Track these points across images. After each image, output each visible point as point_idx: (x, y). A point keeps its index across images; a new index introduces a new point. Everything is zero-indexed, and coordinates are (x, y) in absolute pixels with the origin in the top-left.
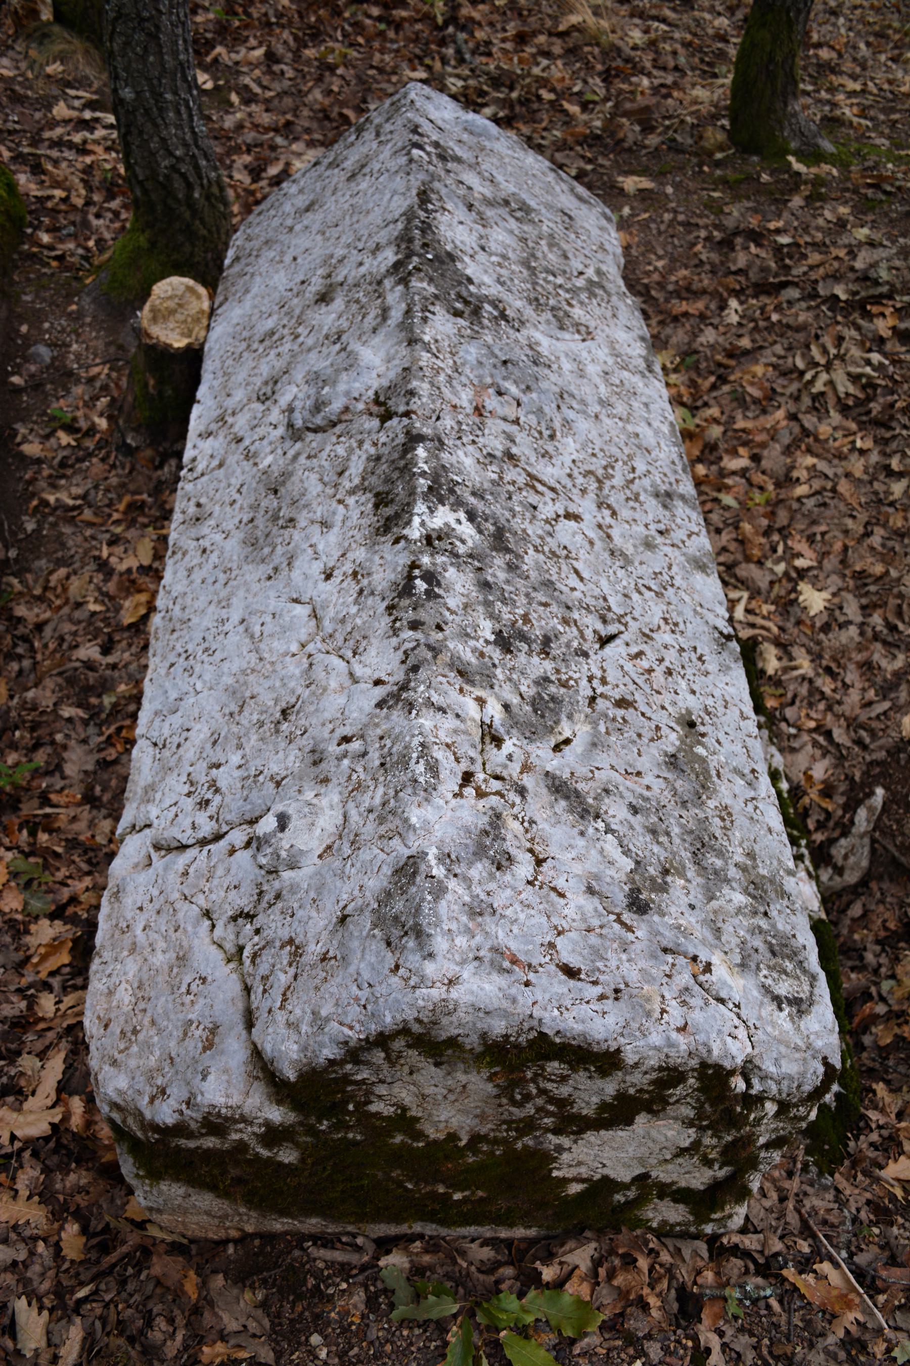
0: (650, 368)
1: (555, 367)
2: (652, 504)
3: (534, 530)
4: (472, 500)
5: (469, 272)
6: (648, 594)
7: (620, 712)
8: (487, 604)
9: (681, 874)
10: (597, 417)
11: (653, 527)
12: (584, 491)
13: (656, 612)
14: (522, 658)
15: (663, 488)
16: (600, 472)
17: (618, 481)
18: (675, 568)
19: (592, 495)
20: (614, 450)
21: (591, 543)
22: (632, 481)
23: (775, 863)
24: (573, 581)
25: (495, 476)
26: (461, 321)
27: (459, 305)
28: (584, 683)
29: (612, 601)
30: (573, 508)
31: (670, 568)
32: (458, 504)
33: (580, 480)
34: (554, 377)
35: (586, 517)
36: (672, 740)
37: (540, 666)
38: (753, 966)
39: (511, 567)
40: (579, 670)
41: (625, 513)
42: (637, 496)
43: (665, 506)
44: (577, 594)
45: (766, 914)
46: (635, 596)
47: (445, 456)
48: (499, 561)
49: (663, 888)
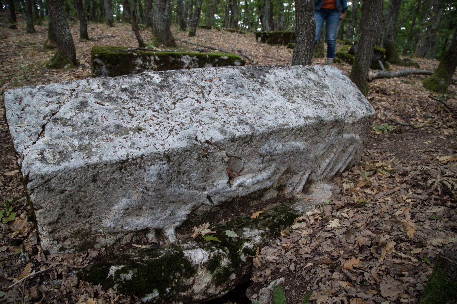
23: (101, 153)
38: (51, 147)
45: (75, 151)
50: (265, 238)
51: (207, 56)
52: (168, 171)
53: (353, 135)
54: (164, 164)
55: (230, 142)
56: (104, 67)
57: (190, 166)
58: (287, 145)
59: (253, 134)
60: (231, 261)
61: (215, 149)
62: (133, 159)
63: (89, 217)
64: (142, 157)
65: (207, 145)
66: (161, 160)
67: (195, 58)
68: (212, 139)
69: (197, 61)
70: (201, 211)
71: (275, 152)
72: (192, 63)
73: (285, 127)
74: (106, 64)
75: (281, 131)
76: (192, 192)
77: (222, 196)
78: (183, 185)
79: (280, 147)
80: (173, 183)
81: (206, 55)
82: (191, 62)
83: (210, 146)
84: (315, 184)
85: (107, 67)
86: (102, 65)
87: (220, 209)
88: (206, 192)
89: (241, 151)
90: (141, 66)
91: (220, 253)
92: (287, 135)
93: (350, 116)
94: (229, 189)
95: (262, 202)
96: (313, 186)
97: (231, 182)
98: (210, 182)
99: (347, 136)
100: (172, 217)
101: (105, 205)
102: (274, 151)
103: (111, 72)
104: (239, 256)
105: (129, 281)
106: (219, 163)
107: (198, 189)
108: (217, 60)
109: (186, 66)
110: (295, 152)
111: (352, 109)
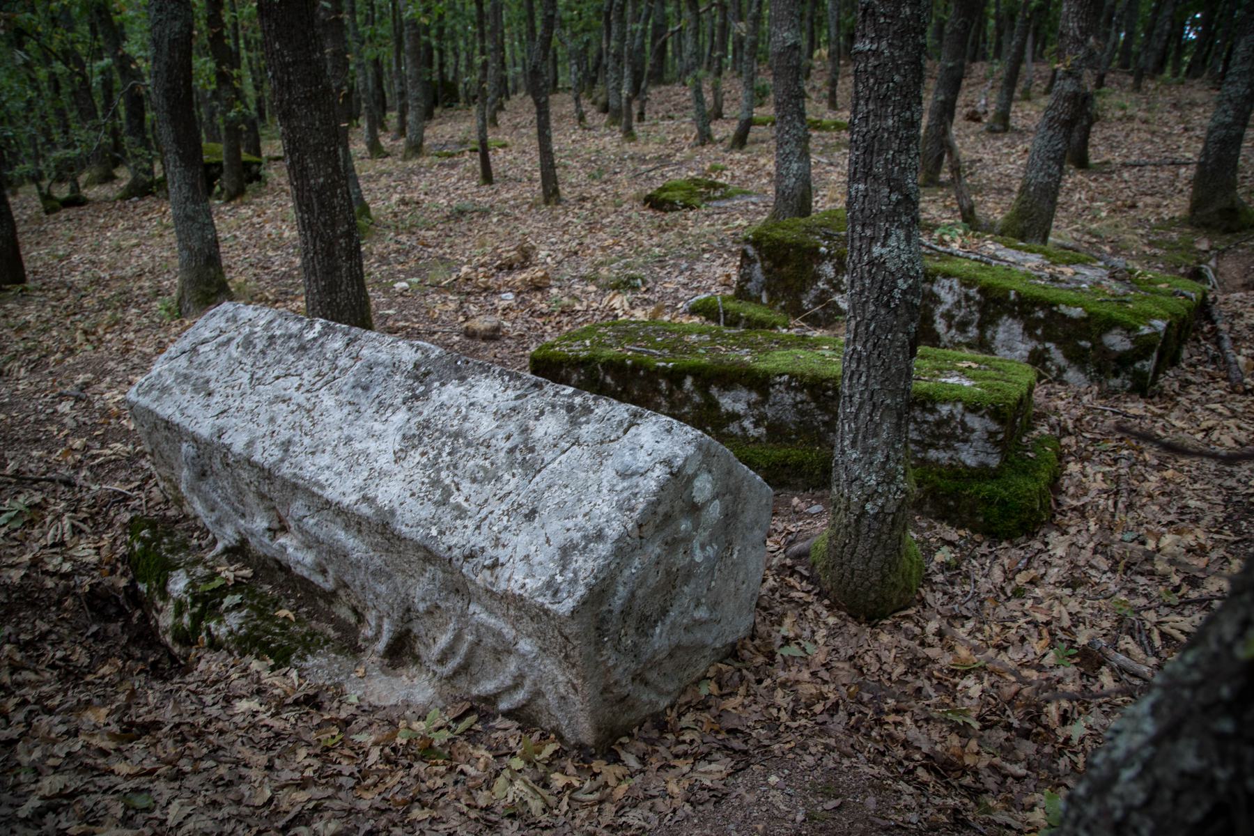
0: (365, 499)
1: (377, 416)
5: (449, 386)
9: (187, 368)
11: (277, 429)
12: (308, 400)
13: (248, 405)
15: (291, 449)
20: (318, 428)
24: (276, 373)
26: (410, 367)
27: (423, 369)
29: (261, 387)
30: (303, 389)
32: (321, 335)
33: (313, 400)
34: (370, 411)
35: (296, 394)
36: (212, 385)
37: (260, 347)
39: (292, 349)
40: (249, 361)
41: (290, 418)
42: (293, 428)
46: (257, 399)
51: (1012, 292)
56: (759, 265)
67: (973, 292)
69: (978, 303)
72: (963, 304)
73: (315, 489)
74: (763, 260)
79: (312, 521)
81: (1007, 291)
82: (959, 302)
84: (421, 672)
85: (763, 267)
86: (755, 261)
90: (829, 282)
93: (484, 567)
96: (414, 670)
97: (278, 535)
103: (768, 279)
107: (236, 510)
108: (1041, 314)
109: (942, 309)
111: (502, 554)
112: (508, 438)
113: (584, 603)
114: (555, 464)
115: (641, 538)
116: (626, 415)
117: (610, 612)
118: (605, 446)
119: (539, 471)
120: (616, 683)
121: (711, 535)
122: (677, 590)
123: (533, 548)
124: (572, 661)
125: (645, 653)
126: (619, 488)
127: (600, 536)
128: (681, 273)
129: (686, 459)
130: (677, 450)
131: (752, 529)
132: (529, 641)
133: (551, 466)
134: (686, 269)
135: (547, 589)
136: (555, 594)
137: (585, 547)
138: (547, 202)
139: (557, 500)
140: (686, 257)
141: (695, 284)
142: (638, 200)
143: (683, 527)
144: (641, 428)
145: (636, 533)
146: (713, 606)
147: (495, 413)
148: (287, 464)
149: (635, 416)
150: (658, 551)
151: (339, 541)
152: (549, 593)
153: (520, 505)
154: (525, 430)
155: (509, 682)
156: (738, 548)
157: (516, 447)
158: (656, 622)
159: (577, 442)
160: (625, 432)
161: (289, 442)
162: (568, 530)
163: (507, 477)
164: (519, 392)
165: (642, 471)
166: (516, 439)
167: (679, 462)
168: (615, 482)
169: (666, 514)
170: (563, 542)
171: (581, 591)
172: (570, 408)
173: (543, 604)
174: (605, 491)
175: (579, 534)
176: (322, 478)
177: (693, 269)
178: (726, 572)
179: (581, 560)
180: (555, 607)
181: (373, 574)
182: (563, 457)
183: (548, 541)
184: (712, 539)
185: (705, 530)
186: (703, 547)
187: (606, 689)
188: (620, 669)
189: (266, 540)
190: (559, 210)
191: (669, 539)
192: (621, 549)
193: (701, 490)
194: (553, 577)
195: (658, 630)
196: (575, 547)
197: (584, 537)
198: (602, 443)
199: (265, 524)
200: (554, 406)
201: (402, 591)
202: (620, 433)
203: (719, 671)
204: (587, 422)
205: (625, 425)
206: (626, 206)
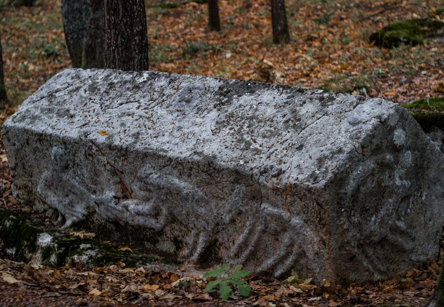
0: (195, 153)
1: (197, 115)
2: (136, 130)
3: (137, 96)
4: (149, 82)
6: (108, 119)
7: (84, 103)
8: (121, 82)
9: (49, 105)
10: (173, 123)
13: (102, 119)
14: (106, 87)
15: (140, 137)
16: (152, 119)
17: (147, 123)
18: (112, 129)
19: (145, 115)
21: (129, 109)
22: (145, 127)
24: (120, 102)
25: (156, 89)
26: (216, 89)
28: (94, 98)
30: (141, 108)
31: (113, 128)
32: (148, 79)
33: (150, 112)
34: (192, 114)
37: (103, 90)
39: (128, 89)
40: (97, 98)
41: (135, 123)
43: (134, 135)
44: (116, 102)
46: (109, 116)
47: (164, 78)
48: (131, 86)
49: (49, 101)
50: (90, 261)
52: (62, 155)
53: (285, 214)
54: (62, 148)
55: (108, 148)
57: (81, 160)
58: (164, 179)
59: (127, 148)
60: (57, 260)
61: (97, 150)
62: (45, 135)
63: (31, 176)
64: (51, 135)
65: (91, 144)
66: (61, 144)
68: (96, 139)
70: (97, 219)
71: (147, 180)
73: (161, 153)
75: (157, 157)
76: (81, 188)
77: (108, 210)
78: (77, 178)
79: (155, 176)
80: (71, 172)
83: (94, 147)
87: (116, 230)
88: (93, 196)
89: (120, 164)
91: (54, 247)
92: (167, 166)
93: (273, 176)
94: (113, 205)
95: (157, 249)
98: (99, 187)
99: (269, 209)
100: (70, 207)
101: (38, 170)
102: (146, 177)
104: (65, 262)
105: (6, 228)
106: (102, 168)
107: (89, 189)
110: (174, 192)
112: (284, 116)
113: (332, 182)
114: (314, 125)
115: (363, 155)
116: (355, 99)
117: (346, 194)
118: (342, 114)
119: (304, 129)
120: (348, 242)
121: (406, 174)
122: (385, 200)
123: (302, 161)
124: (323, 222)
125: (365, 230)
126: (350, 130)
127: (340, 151)
128: (401, 85)
129: (389, 115)
130: (384, 111)
131: (435, 184)
132: (298, 217)
133: (311, 126)
134: (406, 82)
135: (311, 178)
136: (315, 179)
137: (332, 156)
138: (276, 41)
139: (315, 139)
140: (406, 74)
141: (413, 92)
142: (364, 39)
143: (388, 157)
144: (363, 105)
145: (360, 150)
146: (410, 226)
147: (275, 106)
148: (138, 144)
149: (360, 100)
150: (373, 166)
151: (175, 184)
152: (312, 180)
153: (293, 145)
154: (294, 112)
155: (283, 253)
156: (425, 193)
157: (289, 120)
158: (372, 215)
159: (326, 114)
160: (354, 107)
161: (138, 133)
162: (322, 151)
163: (284, 133)
164: (289, 95)
165: (364, 121)
166: (289, 116)
167: (385, 116)
168: (348, 128)
169: (377, 145)
170: (319, 156)
171: (330, 175)
172: (321, 99)
173: (308, 185)
174: (343, 132)
175: (328, 152)
176: (165, 147)
177: (411, 82)
178: (418, 207)
179: (329, 163)
180: (315, 185)
181: (197, 201)
182: (318, 121)
183: (310, 157)
184: (406, 176)
185: (402, 168)
186: (401, 178)
187: (341, 247)
188: (351, 234)
189: (113, 205)
190: (289, 47)
191: (380, 161)
192: (352, 158)
193: (399, 137)
194: (314, 172)
195: (373, 219)
196: (326, 157)
197: (331, 153)
198: (341, 113)
199: (113, 194)
200: (311, 99)
201: (215, 211)
202: (352, 108)
203: (415, 273)
204: (332, 104)
205: (355, 104)
206: (351, 44)
